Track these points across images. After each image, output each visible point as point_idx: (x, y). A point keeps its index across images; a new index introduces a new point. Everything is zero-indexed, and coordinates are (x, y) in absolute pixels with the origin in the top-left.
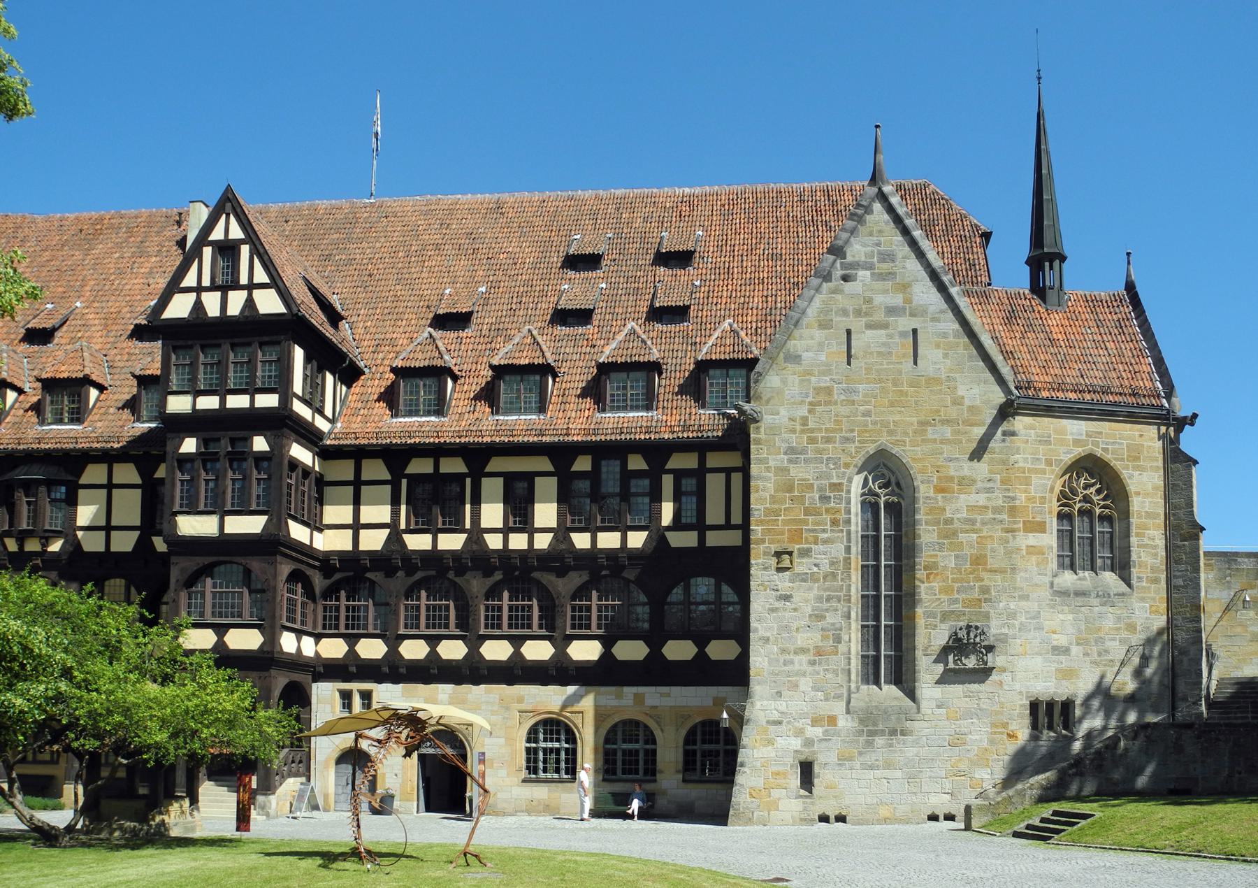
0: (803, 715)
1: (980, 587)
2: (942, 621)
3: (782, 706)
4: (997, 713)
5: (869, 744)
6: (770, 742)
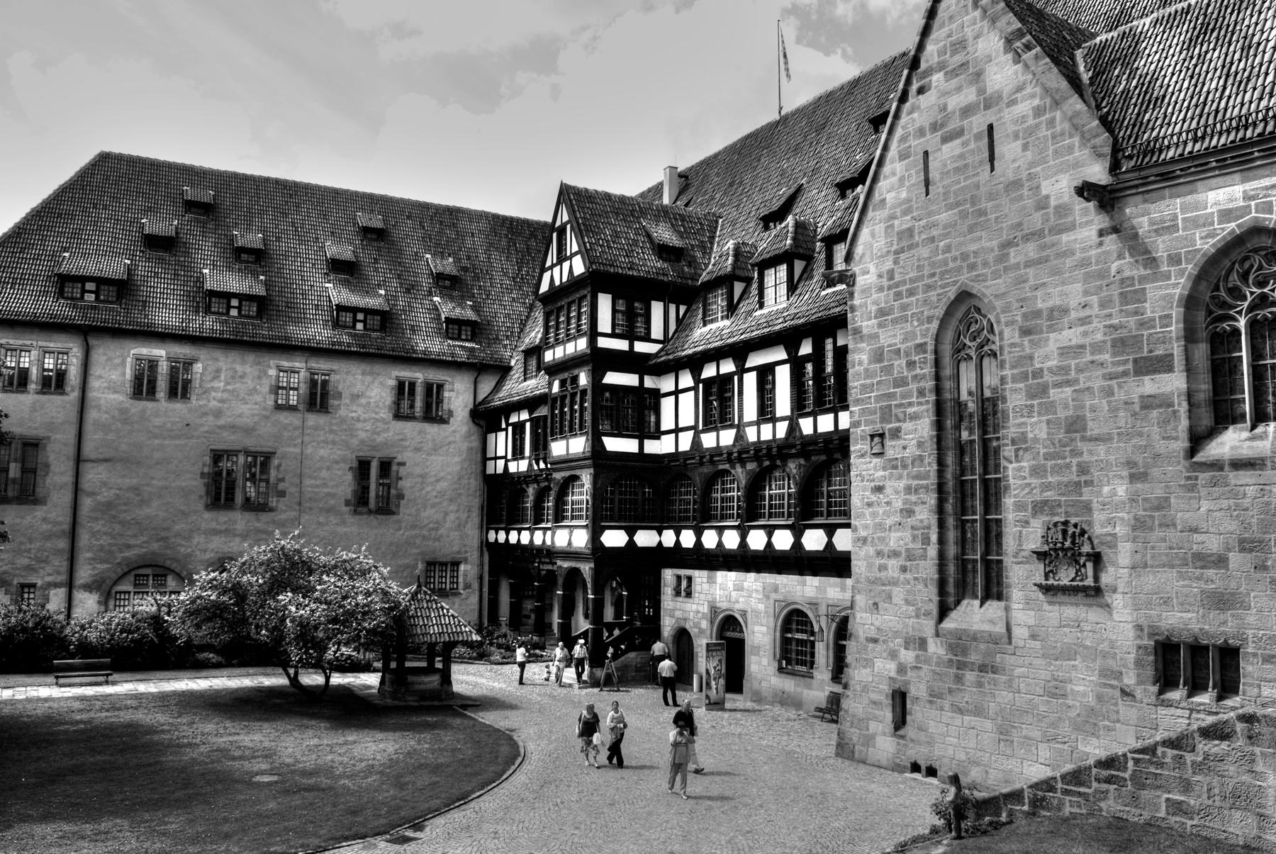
0: (896, 634)
1: (1079, 465)
2: (1034, 515)
3: (878, 620)
4: (1105, 655)
5: (959, 679)
6: (869, 663)
